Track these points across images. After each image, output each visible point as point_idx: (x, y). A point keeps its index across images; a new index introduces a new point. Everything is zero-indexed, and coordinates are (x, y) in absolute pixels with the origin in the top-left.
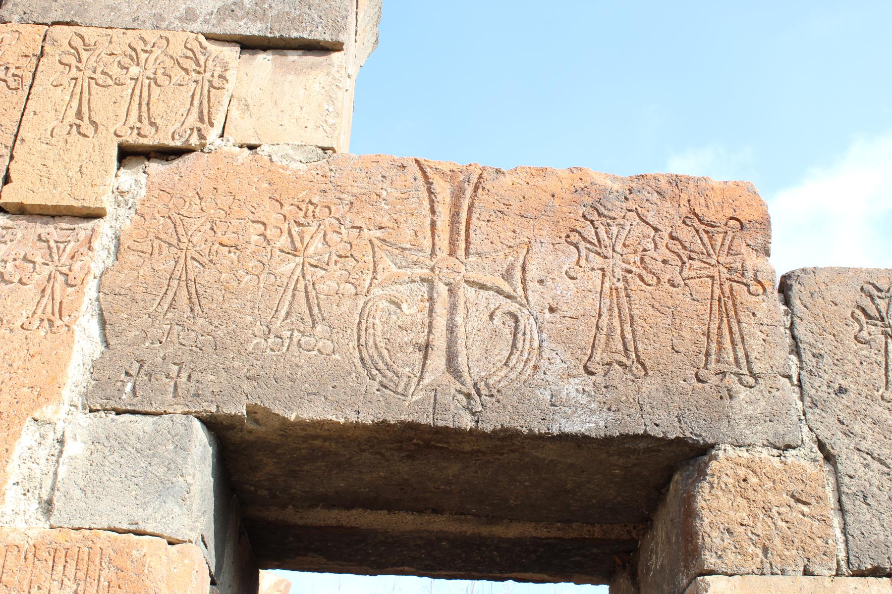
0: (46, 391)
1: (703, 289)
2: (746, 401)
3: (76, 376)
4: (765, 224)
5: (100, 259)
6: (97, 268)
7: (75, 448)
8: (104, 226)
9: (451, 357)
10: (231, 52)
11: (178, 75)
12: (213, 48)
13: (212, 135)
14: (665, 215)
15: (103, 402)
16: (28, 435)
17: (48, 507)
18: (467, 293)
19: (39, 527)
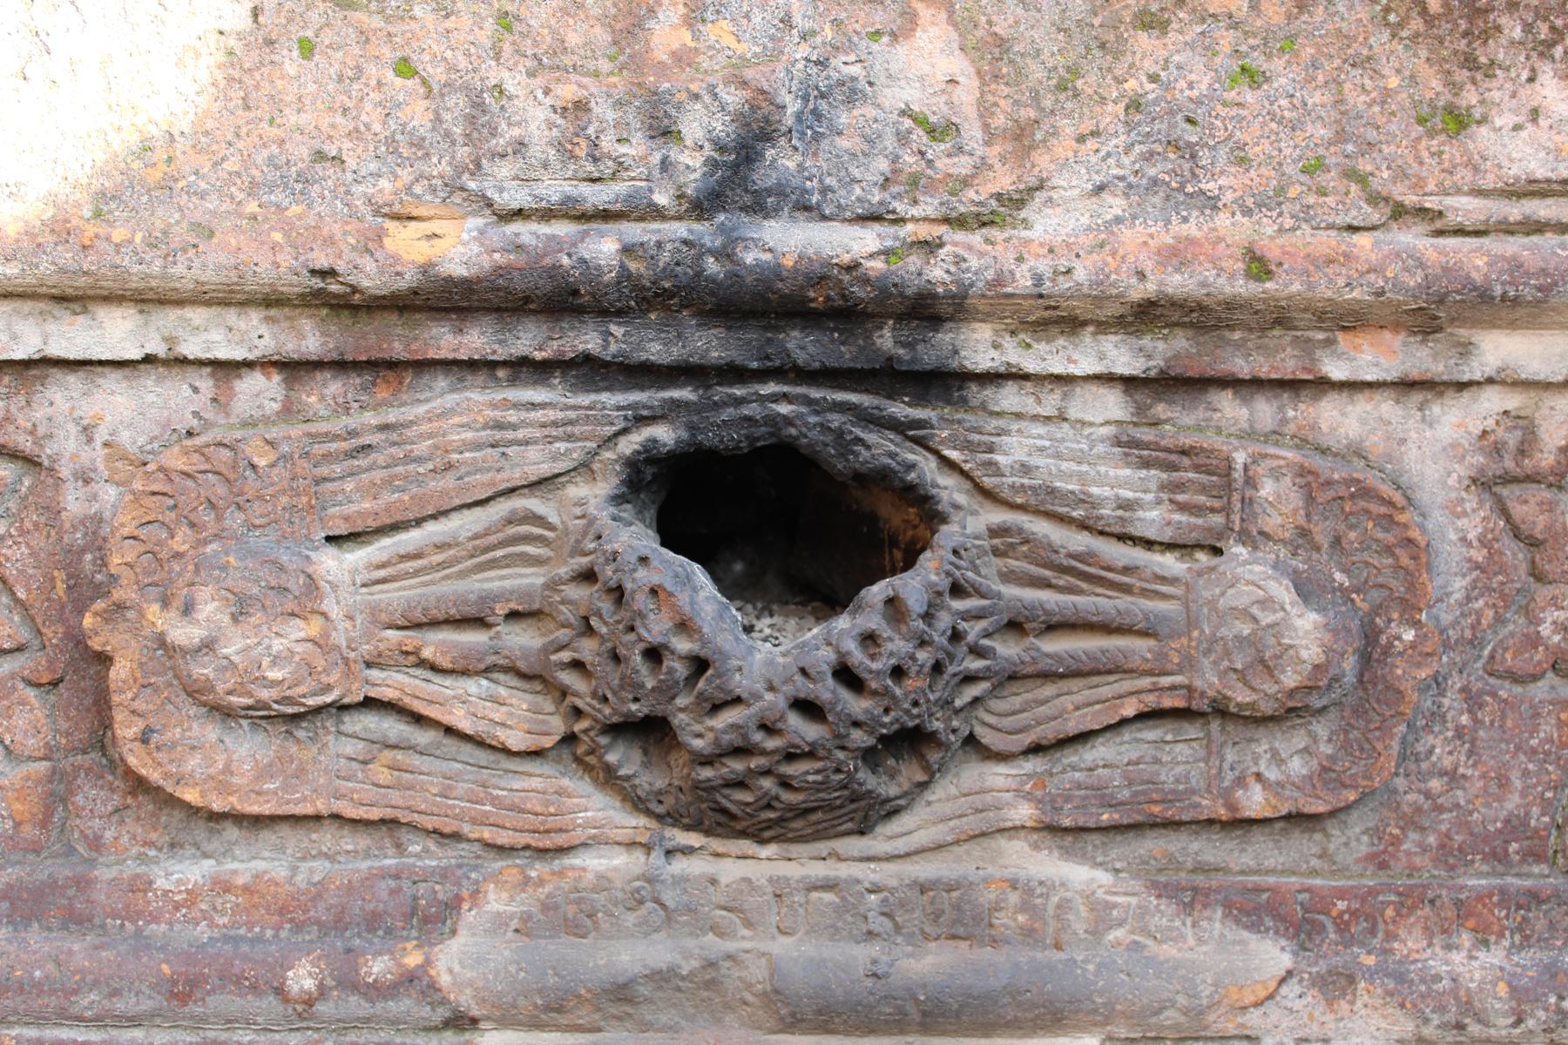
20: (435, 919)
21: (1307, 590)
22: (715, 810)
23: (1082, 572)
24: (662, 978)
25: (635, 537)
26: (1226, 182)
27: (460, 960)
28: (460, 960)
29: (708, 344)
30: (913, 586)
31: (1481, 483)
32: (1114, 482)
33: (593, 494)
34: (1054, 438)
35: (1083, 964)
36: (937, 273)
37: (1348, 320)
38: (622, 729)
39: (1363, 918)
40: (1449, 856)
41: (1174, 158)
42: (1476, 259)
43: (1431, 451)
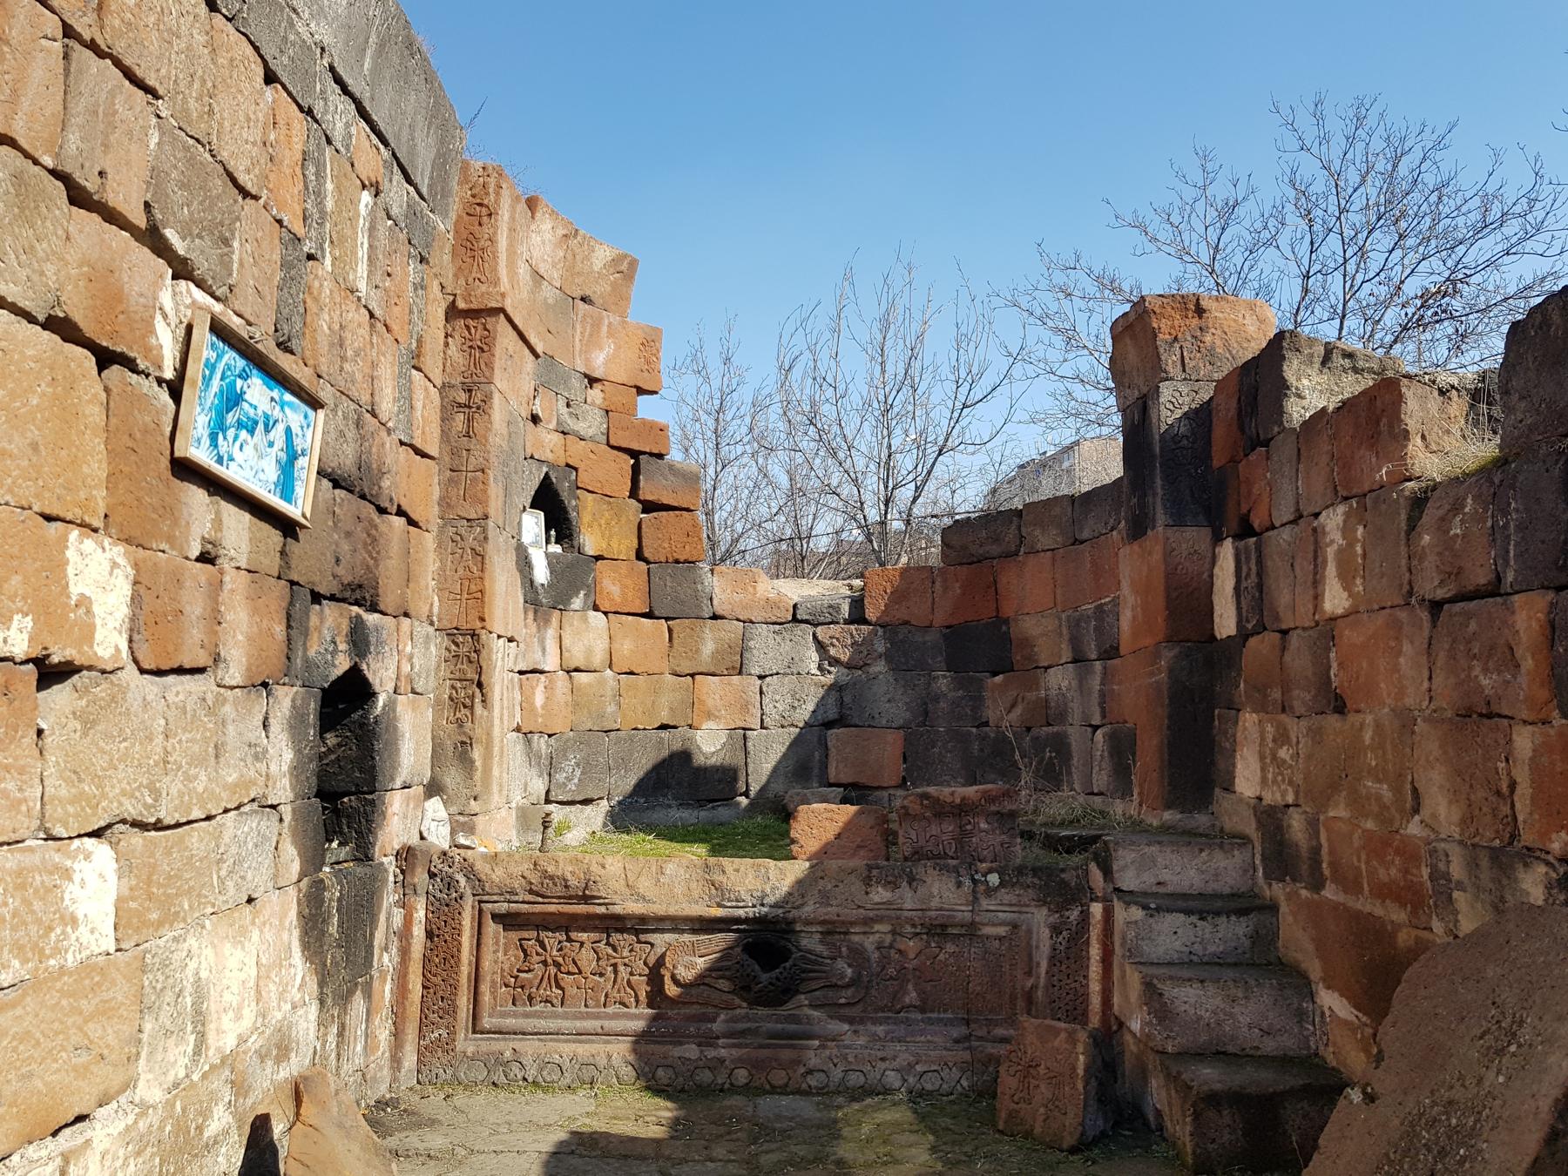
20: (714, 1020)
21: (850, 966)
22: (755, 1002)
23: (815, 962)
24: (749, 1029)
25: (746, 957)
26: (834, 902)
27: (717, 1027)
28: (717, 1027)
29: (756, 927)
30: (787, 965)
31: (878, 948)
32: (820, 948)
33: (739, 950)
34: (811, 941)
35: (816, 1029)
36: (790, 915)
37: (852, 924)
38: (742, 988)
39: (862, 1021)
40: (876, 1011)
41: (825, 899)
42: (871, 914)
43: (869, 943)
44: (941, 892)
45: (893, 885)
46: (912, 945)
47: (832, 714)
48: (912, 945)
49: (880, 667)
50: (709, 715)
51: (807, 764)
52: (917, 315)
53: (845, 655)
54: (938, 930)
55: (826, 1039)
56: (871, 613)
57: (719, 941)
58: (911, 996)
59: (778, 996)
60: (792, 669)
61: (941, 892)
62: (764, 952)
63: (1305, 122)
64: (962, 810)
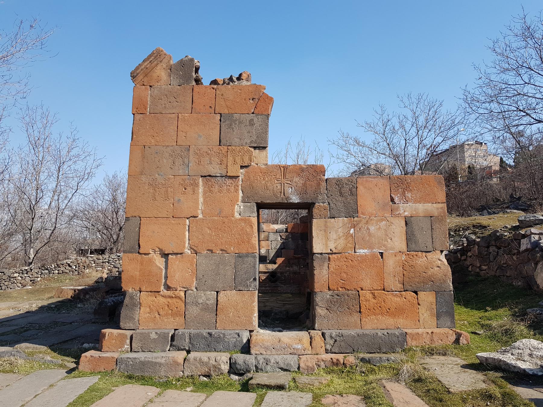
0: (237, 201)
1: (316, 182)
2: (320, 197)
3: (240, 198)
4: (325, 171)
5: (240, 183)
6: (240, 184)
7: (242, 207)
8: (240, 178)
9: (284, 193)
10: (252, 149)
11: (246, 154)
12: (250, 149)
13: (252, 164)
14: (311, 171)
15: (244, 201)
16: (236, 206)
17: (240, 214)
18: (286, 184)
19: (240, 217)
34: (279, 275)
44: (295, 268)
45: (289, 267)
46: (292, 275)
47: (283, 247)
48: (292, 275)
49: (290, 240)
50: (263, 247)
51: (278, 254)
52: (306, 153)
53: (284, 238)
54: (295, 273)
55: (281, 287)
56: (289, 231)
57: (267, 274)
58: (292, 282)
59: (275, 282)
60: (276, 240)
61: (295, 268)
62: (272, 276)
63: (405, 100)
64: (299, 258)
